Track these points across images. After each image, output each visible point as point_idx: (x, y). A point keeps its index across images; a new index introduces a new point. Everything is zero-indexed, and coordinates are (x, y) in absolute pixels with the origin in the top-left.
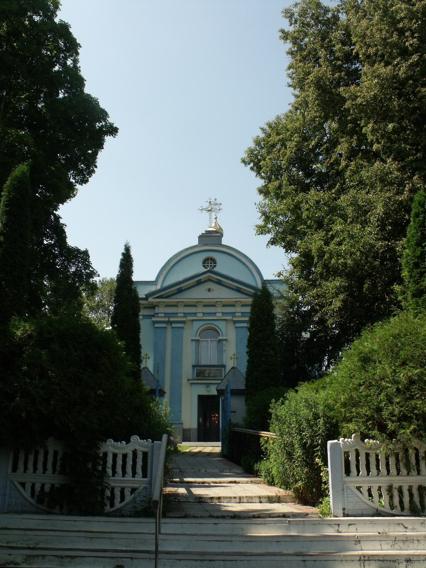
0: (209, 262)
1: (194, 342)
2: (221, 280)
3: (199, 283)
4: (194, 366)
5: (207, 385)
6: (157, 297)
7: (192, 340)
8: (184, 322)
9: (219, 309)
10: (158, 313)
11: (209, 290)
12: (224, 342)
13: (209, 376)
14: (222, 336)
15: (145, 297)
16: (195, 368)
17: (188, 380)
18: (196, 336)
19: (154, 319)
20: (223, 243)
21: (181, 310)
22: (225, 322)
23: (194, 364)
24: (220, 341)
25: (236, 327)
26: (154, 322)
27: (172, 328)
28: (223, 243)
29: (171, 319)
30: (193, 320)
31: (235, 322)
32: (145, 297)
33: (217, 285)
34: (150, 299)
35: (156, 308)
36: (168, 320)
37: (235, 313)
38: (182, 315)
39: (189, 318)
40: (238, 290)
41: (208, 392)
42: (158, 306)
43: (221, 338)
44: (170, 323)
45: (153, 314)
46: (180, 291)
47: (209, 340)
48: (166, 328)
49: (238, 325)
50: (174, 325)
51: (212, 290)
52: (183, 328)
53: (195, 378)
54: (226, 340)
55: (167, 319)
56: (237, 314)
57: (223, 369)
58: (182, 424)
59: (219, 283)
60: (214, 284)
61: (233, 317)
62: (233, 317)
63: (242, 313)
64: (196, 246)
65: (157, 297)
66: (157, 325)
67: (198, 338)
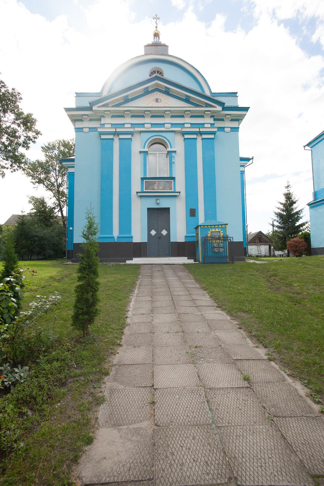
0: (157, 75)
1: (142, 154)
2: (169, 89)
3: (147, 92)
4: (142, 179)
5: (157, 198)
6: (104, 106)
7: (140, 152)
8: (132, 133)
9: (168, 120)
10: (104, 124)
11: (157, 100)
12: (173, 154)
13: (158, 189)
14: (171, 148)
15: (89, 105)
16: (144, 181)
17: (137, 193)
18: (144, 148)
19: (99, 130)
20: (170, 53)
21: (128, 120)
22: (174, 133)
23: (143, 177)
24: (169, 152)
25: (185, 139)
26: (101, 134)
27: (119, 139)
28: (170, 53)
29: (118, 130)
30: (141, 132)
31: (183, 134)
32: (89, 105)
33: (164, 95)
34: (94, 108)
35: (102, 119)
36: (115, 131)
37: (184, 124)
38: (130, 126)
39: (137, 129)
40: (187, 100)
41: (158, 204)
42: (104, 117)
43: (169, 149)
44: (116, 134)
45: (100, 126)
46: (127, 100)
47: (158, 153)
48: (113, 139)
49: (186, 136)
50: (121, 137)
51: (159, 100)
52: (131, 139)
53: (144, 191)
54: (175, 152)
55: (114, 130)
56: (186, 126)
57: (173, 181)
58: (132, 237)
59: (167, 92)
60: (162, 94)
61: (182, 128)
62: (182, 128)
63: (191, 124)
64: (142, 56)
65: (104, 106)
66: (103, 137)
67: (146, 149)
